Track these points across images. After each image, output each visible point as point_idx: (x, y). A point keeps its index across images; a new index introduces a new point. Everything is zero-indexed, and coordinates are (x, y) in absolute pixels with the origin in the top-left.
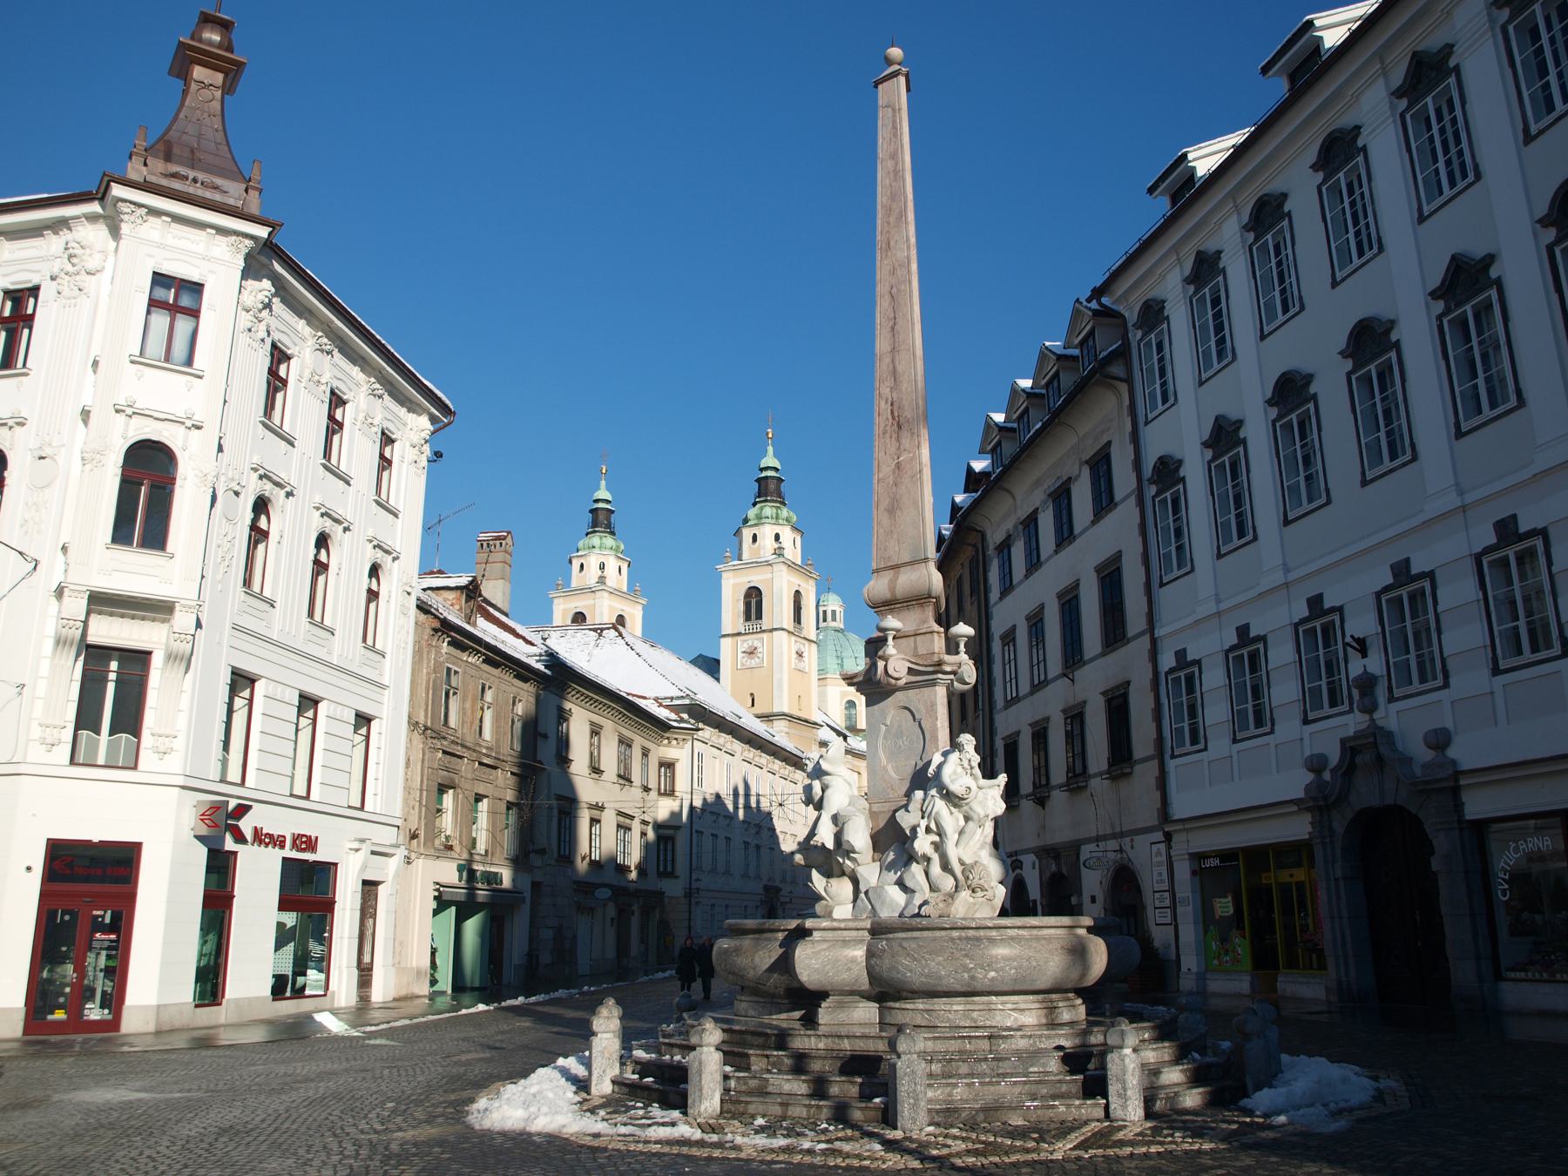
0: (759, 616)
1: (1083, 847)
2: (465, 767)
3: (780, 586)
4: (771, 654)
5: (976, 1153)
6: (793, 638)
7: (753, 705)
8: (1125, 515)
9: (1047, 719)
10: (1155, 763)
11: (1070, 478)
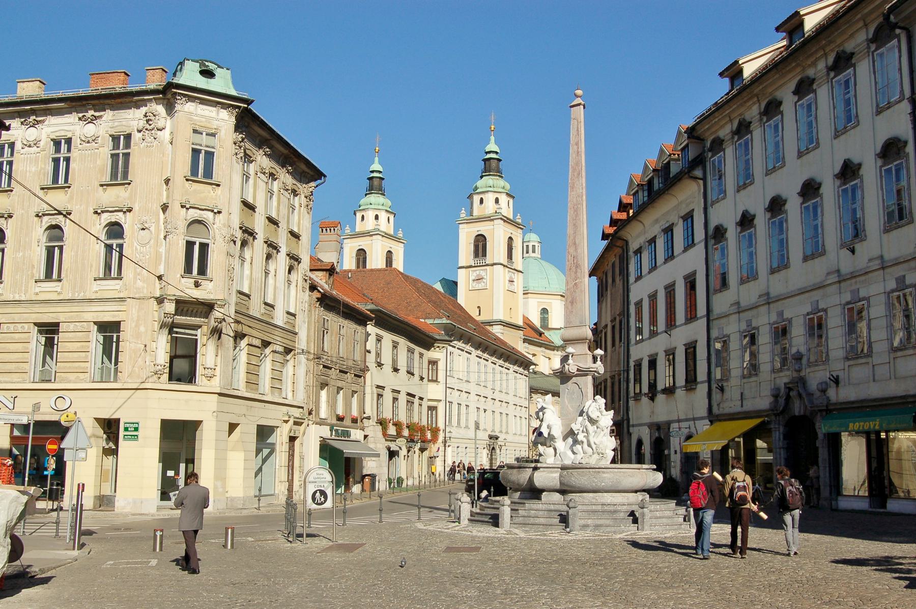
0: (484, 255)
1: (672, 425)
2: (333, 373)
3: (498, 235)
4: (492, 280)
5: (593, 536)
6: (507, 269)
7: (480, 314)
8: (698, 251)
9: (657, 354)
10: (706, 384)
11: (673, 224)
